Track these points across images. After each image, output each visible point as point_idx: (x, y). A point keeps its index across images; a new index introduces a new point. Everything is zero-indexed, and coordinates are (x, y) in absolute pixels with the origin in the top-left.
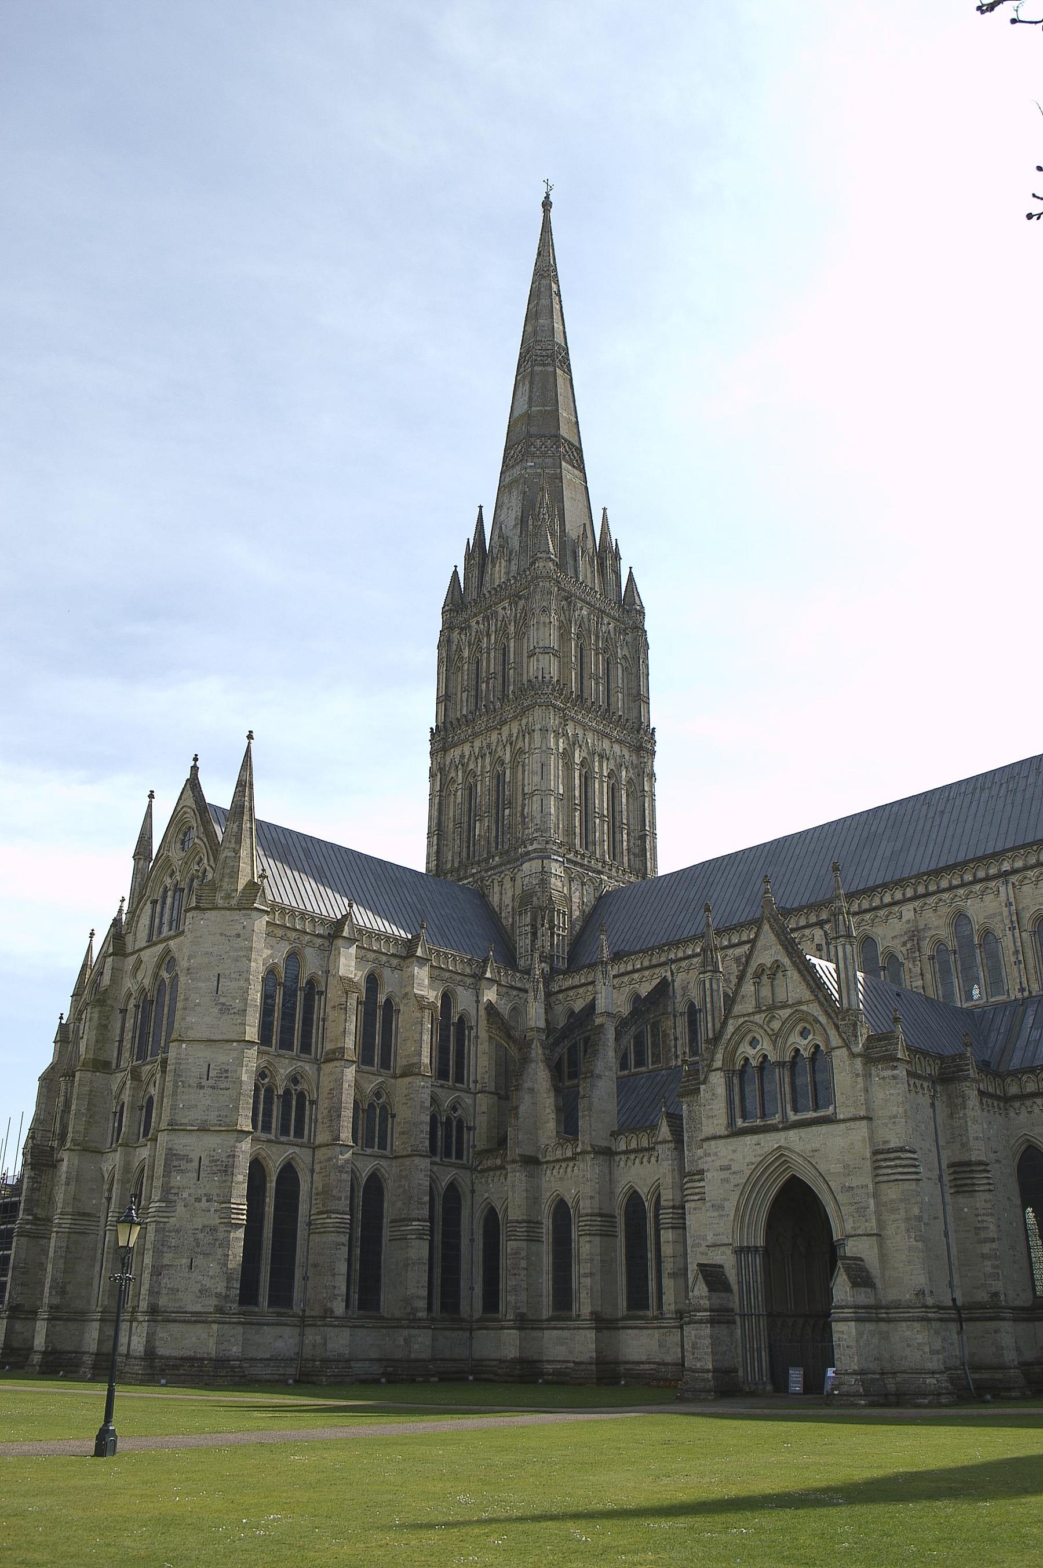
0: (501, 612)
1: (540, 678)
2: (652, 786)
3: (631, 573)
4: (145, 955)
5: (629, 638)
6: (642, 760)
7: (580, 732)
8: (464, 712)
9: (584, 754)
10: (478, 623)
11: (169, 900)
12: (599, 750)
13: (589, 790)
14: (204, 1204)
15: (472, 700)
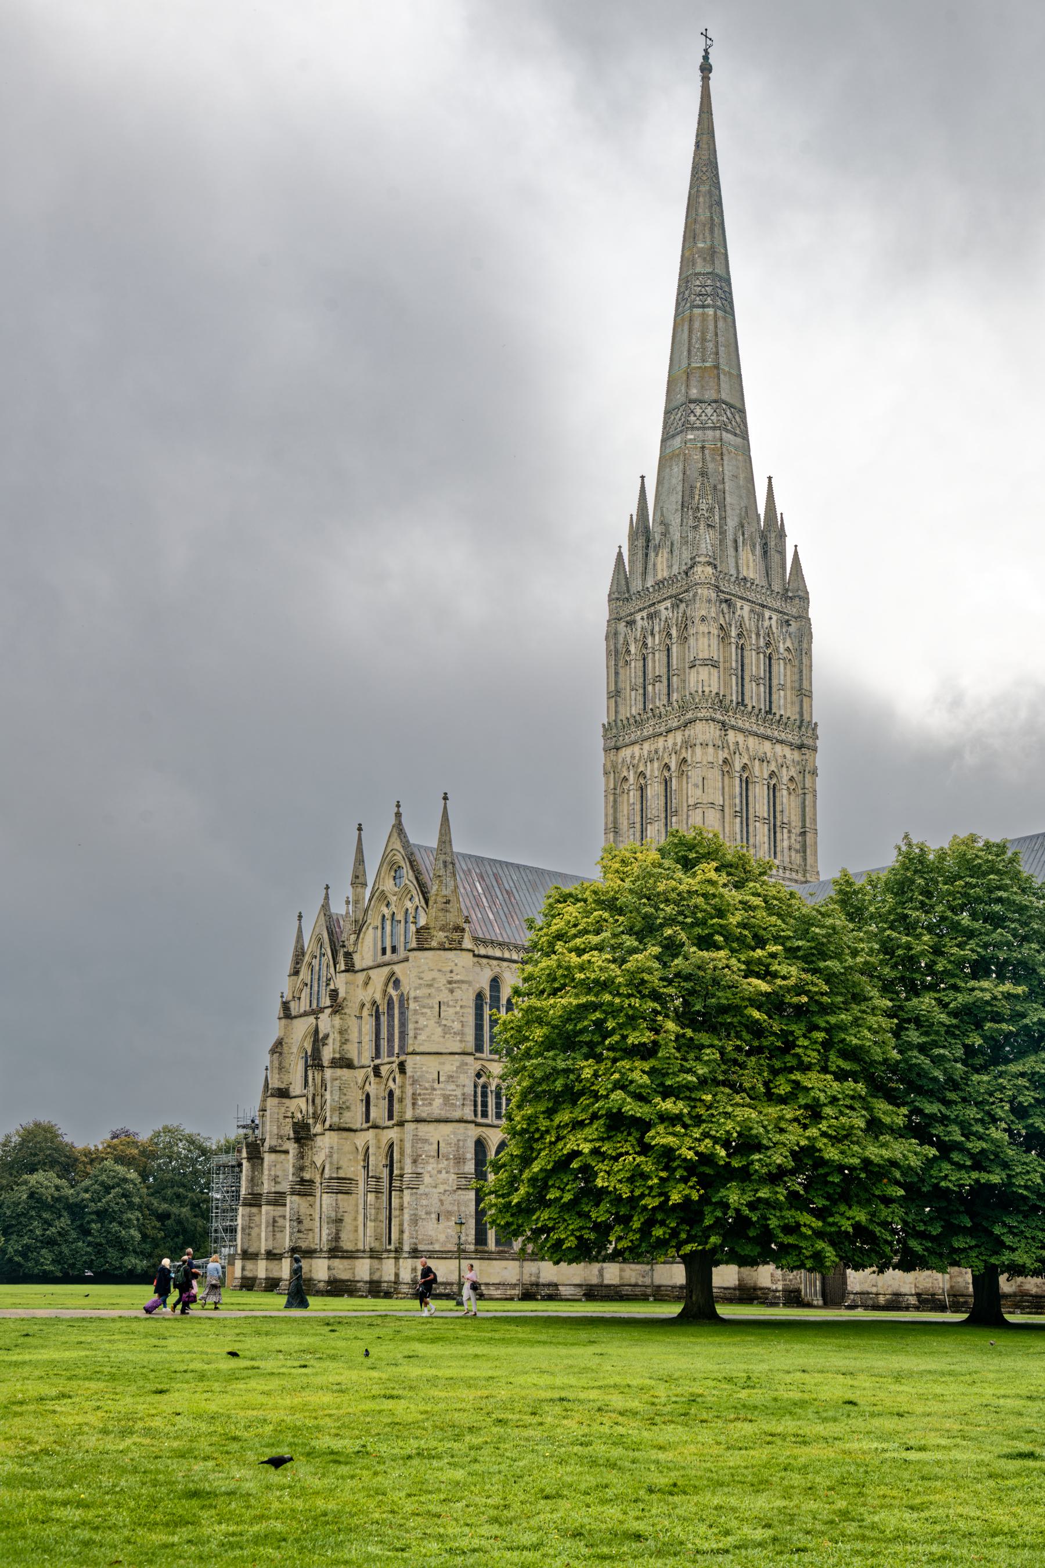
0: (664, 614)
1: (700, 693)
2: (814, 782)
3: (796, 553)
4: (371, 972)
5: (792, 629)
6: (804, 757)
7: (740, 738)
8: (634, 712)
9: (745, 761)
10: (642, 619)
11: (388, 928)
12: (760, 754)
13: (750, 794)
14: (444, 1175)
15: (640, 698)
